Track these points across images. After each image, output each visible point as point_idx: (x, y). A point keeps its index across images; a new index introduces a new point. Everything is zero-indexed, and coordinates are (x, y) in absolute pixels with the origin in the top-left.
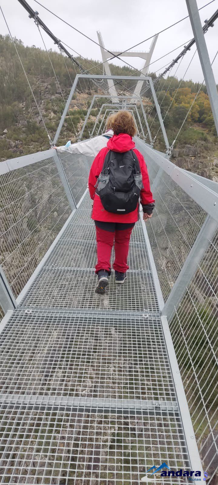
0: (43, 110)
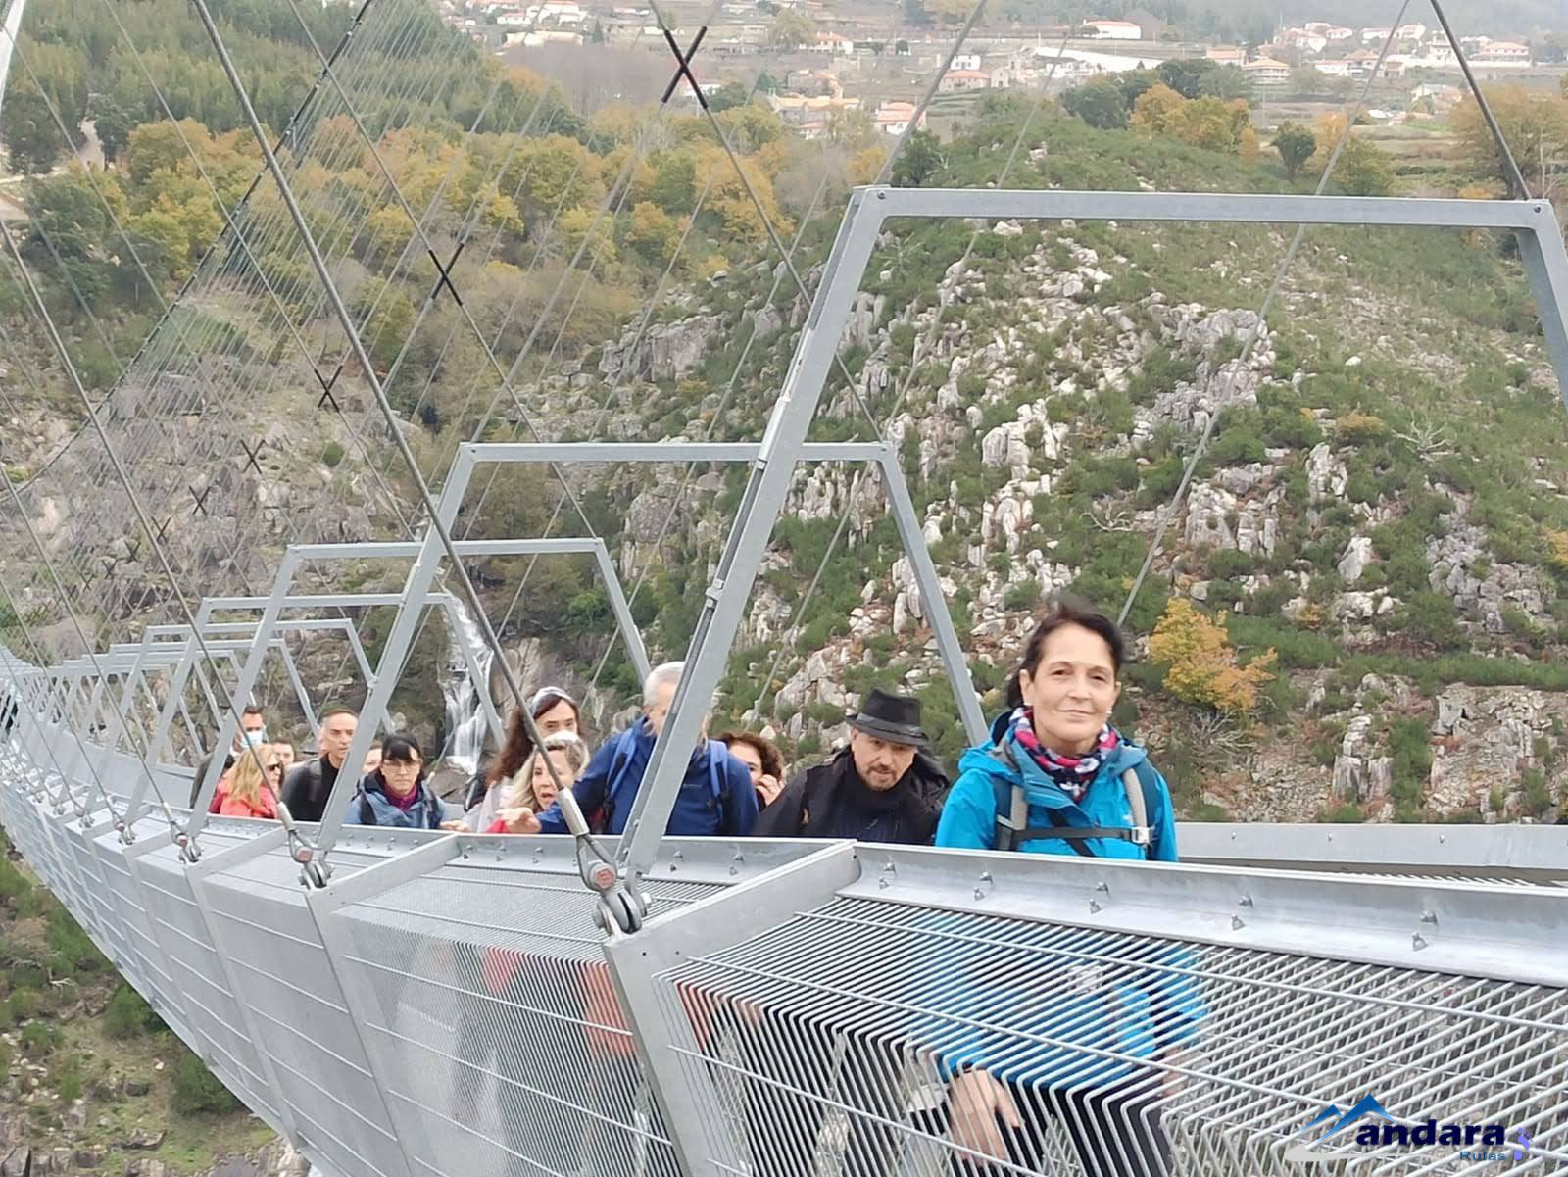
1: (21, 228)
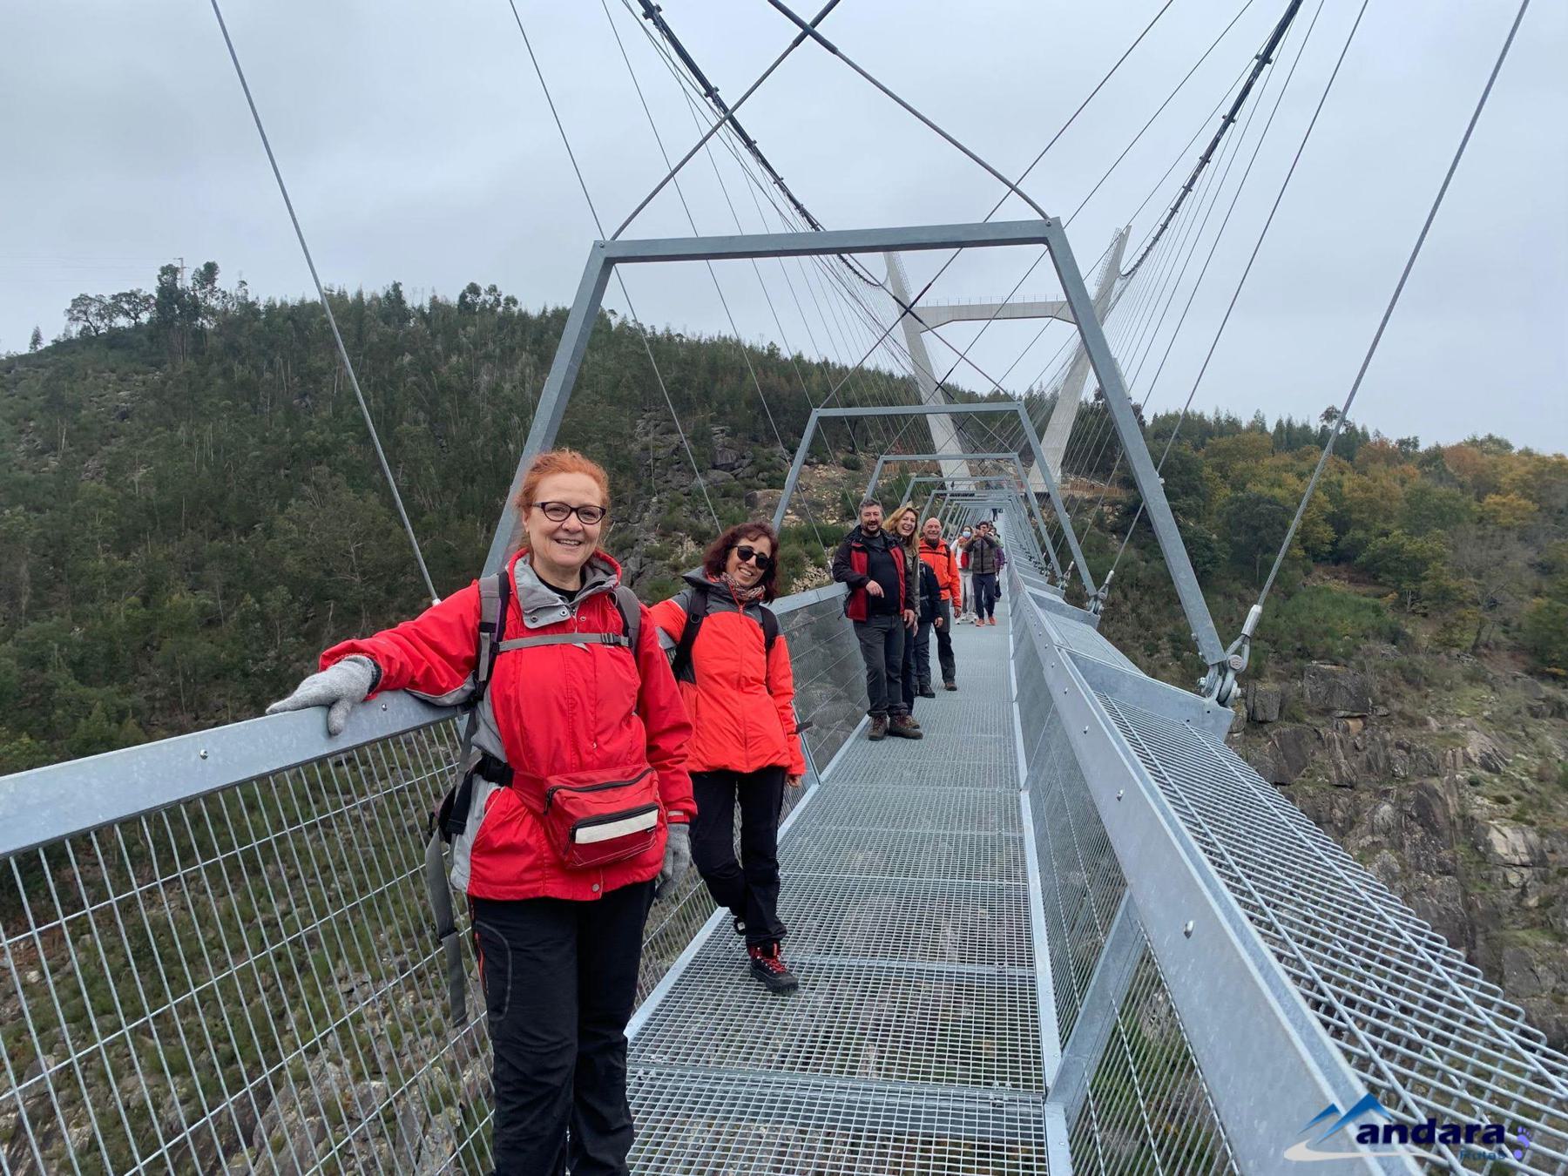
0: (653, 534)
1: (1113, 504)
